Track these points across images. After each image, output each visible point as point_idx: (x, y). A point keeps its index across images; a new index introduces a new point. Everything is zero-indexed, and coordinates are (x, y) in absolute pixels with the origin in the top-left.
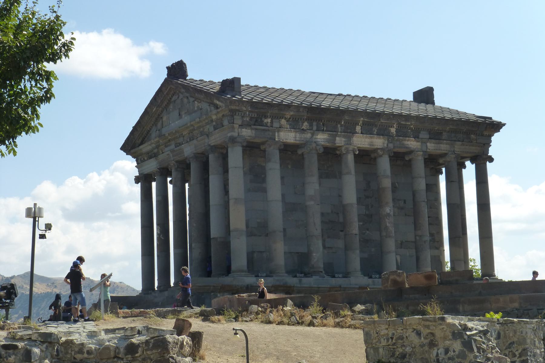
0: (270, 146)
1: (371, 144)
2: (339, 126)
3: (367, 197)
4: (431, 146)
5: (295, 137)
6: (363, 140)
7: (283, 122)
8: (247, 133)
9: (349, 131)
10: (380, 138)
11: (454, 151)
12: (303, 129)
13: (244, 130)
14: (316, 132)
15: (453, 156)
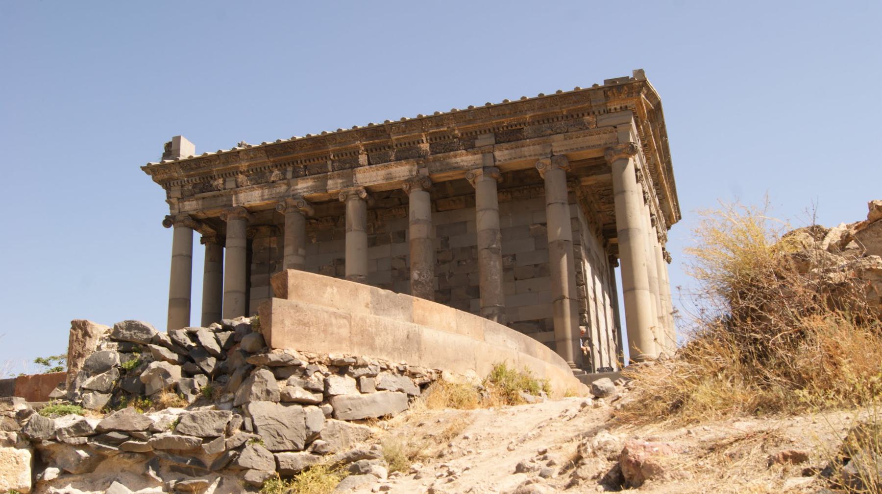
0: (225, 216)
1: (389, 177)
2: (329, 163)
3: (444, 262)
4: (502, 155)
5: (262, 196)
6: (374, 174)
7: (241, 178)
8: (190, 206)
9: (348, 165)
10: (402, 165)
11: (552, 152)
12: (273, 182)
13: (186, 203)
14: (292, 181)
15: (548, 161)
